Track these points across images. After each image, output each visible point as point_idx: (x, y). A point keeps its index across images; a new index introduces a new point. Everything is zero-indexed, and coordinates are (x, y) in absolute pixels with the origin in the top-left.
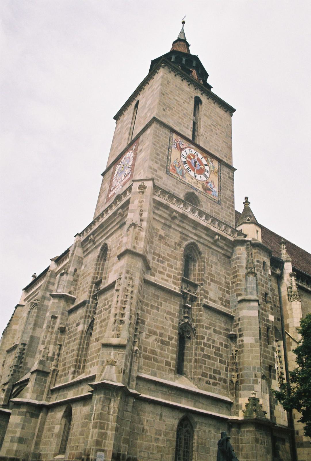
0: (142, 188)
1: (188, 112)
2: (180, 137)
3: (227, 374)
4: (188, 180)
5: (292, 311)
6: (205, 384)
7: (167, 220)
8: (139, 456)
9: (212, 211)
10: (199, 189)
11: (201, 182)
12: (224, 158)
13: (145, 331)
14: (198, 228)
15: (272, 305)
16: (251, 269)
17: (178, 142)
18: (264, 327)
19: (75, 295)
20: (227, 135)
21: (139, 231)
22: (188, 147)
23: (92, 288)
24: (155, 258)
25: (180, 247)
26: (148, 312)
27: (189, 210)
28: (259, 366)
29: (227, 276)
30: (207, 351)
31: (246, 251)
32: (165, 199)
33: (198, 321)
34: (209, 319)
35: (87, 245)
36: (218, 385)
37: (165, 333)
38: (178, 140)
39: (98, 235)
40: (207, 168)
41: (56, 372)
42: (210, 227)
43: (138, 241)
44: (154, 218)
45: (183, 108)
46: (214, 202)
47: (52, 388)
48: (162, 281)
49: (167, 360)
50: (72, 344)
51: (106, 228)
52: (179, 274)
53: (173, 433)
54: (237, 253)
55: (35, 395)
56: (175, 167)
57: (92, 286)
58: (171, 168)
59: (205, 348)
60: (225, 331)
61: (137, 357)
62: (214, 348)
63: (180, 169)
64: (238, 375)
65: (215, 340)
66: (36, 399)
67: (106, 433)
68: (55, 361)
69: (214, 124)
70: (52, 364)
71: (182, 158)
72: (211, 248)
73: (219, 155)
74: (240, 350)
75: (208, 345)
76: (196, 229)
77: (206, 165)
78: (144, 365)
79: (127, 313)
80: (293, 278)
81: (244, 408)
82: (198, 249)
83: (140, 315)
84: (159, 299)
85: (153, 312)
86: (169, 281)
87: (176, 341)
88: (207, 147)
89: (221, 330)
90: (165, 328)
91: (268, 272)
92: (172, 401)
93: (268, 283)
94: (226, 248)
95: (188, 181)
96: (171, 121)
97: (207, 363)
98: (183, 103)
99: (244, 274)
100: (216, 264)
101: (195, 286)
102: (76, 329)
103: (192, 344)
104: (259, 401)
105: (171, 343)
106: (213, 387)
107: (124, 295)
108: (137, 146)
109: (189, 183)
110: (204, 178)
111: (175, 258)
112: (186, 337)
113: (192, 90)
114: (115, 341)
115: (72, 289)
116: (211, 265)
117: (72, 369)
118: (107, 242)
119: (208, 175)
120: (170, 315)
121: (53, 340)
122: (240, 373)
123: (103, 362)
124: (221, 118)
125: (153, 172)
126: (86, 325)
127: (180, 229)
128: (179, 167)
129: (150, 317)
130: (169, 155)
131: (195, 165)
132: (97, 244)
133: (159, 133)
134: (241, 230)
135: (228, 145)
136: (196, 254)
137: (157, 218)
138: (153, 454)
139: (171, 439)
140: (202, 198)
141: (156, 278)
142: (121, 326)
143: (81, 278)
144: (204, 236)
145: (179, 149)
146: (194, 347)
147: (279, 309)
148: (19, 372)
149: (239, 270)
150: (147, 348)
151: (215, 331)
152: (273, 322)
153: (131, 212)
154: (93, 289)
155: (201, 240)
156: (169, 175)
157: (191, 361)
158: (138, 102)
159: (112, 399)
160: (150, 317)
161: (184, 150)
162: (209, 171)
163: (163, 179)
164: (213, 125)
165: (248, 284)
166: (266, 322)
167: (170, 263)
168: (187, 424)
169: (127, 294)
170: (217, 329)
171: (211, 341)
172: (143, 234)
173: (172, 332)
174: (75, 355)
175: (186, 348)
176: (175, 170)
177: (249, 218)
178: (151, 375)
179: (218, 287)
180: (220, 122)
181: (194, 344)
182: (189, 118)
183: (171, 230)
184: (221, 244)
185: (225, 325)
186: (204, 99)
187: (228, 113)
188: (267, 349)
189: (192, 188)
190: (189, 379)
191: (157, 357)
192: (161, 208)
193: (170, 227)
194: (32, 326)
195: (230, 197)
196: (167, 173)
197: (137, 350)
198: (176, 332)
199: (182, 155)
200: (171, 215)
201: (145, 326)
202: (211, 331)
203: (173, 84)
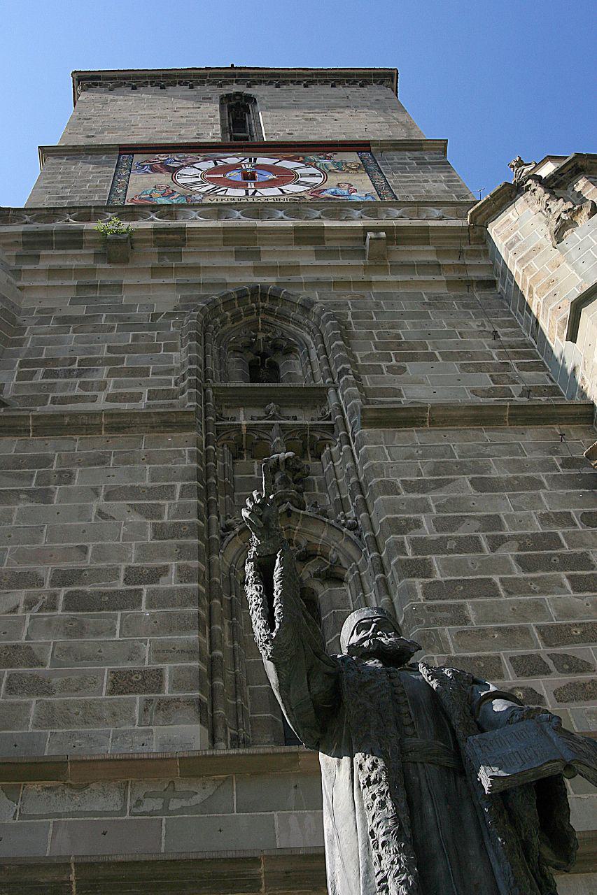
17: (160, 162)
22: (205, 160)
34: (422, 456)
42: (323, 223)
44: (21, 288)
49: (128, 666)
60: (562, 471)
65: (502, 514)
89: (527, 474)
101: (315, 397)
136: (298, 323)
145: (163, 170)
155: (303, 277)
185: (556, 452)
192: (43, 252)
193: (119, 287)
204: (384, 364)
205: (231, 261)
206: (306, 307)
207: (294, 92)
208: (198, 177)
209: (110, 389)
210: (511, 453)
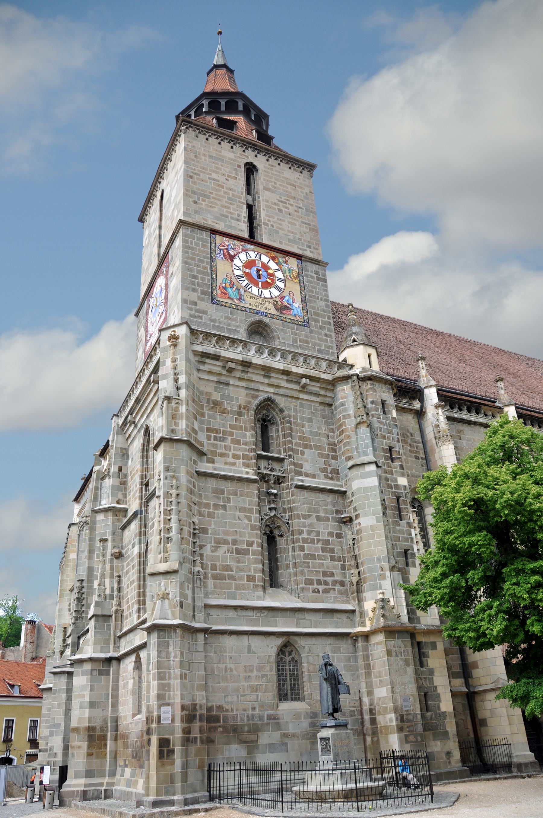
0: (174, 338)
1: (236, 193)
2: (227, 239)
3: (345, 574)
4: (249, 303)
5: (443, 461)
6: (311, 594)
7: (221, 375)
8: (225, 702)
9: (294, 341)
11: (271, 301)
12: (306, 250)
13: (210, 543)
14: (273, 375)
15: (401, 462)
16: (361, 417)
17: (226, 247)
18: (391, 497)
19: (126, 504)
20: (307, 210)
21: (177, 405)
22: (243, 251)
23: (142, 492)
24: (211, 436)
25: (248, 410)
26: (210, 515)
27: (253, 352)
28: (386, 554)
29: (331, 434)
30: (309, 549)
31: (353, 391)
32: (212, 346)
33: (291, 510)
34: (307, 504)
35: (128, 429)
36: (332, 591)
37: (241, 538)
39: (137, 414)
40: (279, 275)
41: (120, 613)
43: (177, 421)
45: (227, 188)
46: (298, 324)
47: (119, 634)
48: (227, 467)
49: (249, 574)
50: (131, 573)
51: (144, 402)
52: (251, 450)
53: (270, 665)
54: (340, 397)
55: (99, 647)
56: (225, 288)
57: (142, 488)
58: (219, 292)
59: (306, 545)
60: (335, 515)
61: (200, 579)
62: (321, 542)
63: (234, 289)
64: (359, 573)
65: (320, 530)
66: (101, 652)
67: (169, 684)
68: (115, 599)
69: (283, 200)
70: (112, 604)
71: (235, 270)
72: (298, 398)
73: (298, 248)
74: (358, 538)
75: (309, 541)
76: (269, 377)
77: (277, 270)
78: (215, 587)
79: (174, 525)
80: (440, 411)
81: (371, 614)
82: (276, 405)
83: (196, 523)
84: (224, 494)
85: (218, 513)
86: (237, 464)
87: (258, 547)
88: (274, 241)
89: (328, 515)
90: (240, 531)
91: (392, 414)
92: (263, 626)
93: (392, 431)
94: (322, 392)
95: (250, 304)
96: (209, 216)
97: (311, 565)
98: (225, 181)
99: (353, 426)
100: (310, 420)
101: (280, 460)
102: (133, 552)
103: (288, 544)
104: (389, 601)
105: (252, 550)
106: (325, 595)
107: (167, 503)
108: (168, 267)
109: (251, 307)
110: (276, 293)
111: (241, 428)
112: (277, 536)
113: (238, 155)
114: (163, 567)
115: (120, 496)
116: (303, 424)
117: (136, 607)
118: (148, 422)
119: (281, 285)
120: (245, 512)
121: (108, 572)
122: (362, 569)
123: (153, 596)
124: (294, 186)
125: (191, 306)
126: (143, 545)
127: (243, 384)
128: (232, 287)
129: (214, 521)
130: (213, 271)
131: (259, 276)
132: (139, 426)
133: (192, 243)
134: (345, 360)
135: (312, 227)
137: (206, 377)
138: (245, 695)
139: (268, 673)
140: (275, 324)
141: (216, 465)
142: (169, 545)
143: (129, 478)
144: (284, 384)
146: (290, 546)
147: (424, 461)
148: (82, 618)
149: (345, 422)
150: (216, 565)
151: (318, 518)
152: (405, 486)
153: (163, 379)
154: (144, 493)
155: (281, 391)
156: (217, 304)
157: (288, 567)
158: (163, 191)
159: (171, 642)
160: (214, 521)
161: (237, 257)
162: (283, 278)
163: (209, 313)
164: (281, 202)
165: (359, 439)
166: (394, 490)
167: (234, 437)
168: (292, 651)
169: (170, 500)
170: (322, 514)
171: (314, 534)
172: (183, 409)
173: (250, 535)
174: (136, 588)
175: (279, 551)
176: (225, 294)
177: (356, 338)
178: (228, 598)
179: (317, 454)
180: (293, 192)
181: (290, 543)
182: (239, 202)
183: (231, 388)
184: (315, 387)
185: (334, 507)
186: (260, 161)
187: (306, 172)
188: (398, 528)
189: (257, 314)
190: (288, 591)
191: (234, 573)
192: (207, 361)
193: (227, 384)
194: (86, 554)
195: (324, 311)
196: (214, 301)
197: (199, 572)
198: (257, 534)
199: (234, 266)
200: (225, 367)
201: (209, 535)
202: (314, 519)
203: (205, 155)
204: (300, 449)
205: (261, 379)
206: (282, 411)
207: (274, 168)
209: (232, 452)
210: (325, 506)
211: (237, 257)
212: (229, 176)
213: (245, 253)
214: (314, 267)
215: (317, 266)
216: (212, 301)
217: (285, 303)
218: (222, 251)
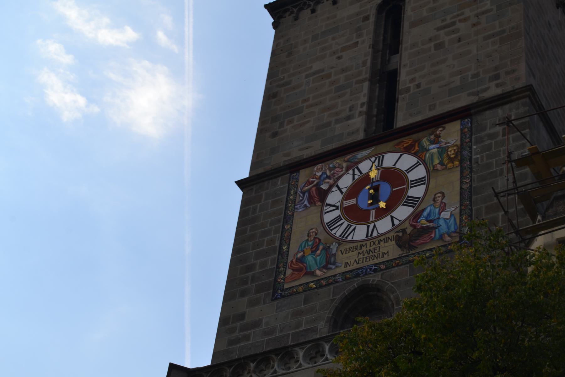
2: (319, 166)
10: (386, 258)
11: (390, 235)
17: (315, 183)
22: (347, 170)
38: (314, 176)
56: (301, 260)
58: (289, 272)
63: (319, 252)
69: (449, 21)
73: (469, 95)
109: (348, 268)
130: (286, 238)
156: (283, 297)
182: (357, 82)
189: (358, 275)
203: (305, 41)
208: (337, 208)
211: (335, 189)
212: (343, 49)
213: (351, 172)
214: (501, 113)
215: (507, 107)
216: (273, 295)
217: (423, 222)
218: (306, 195)
